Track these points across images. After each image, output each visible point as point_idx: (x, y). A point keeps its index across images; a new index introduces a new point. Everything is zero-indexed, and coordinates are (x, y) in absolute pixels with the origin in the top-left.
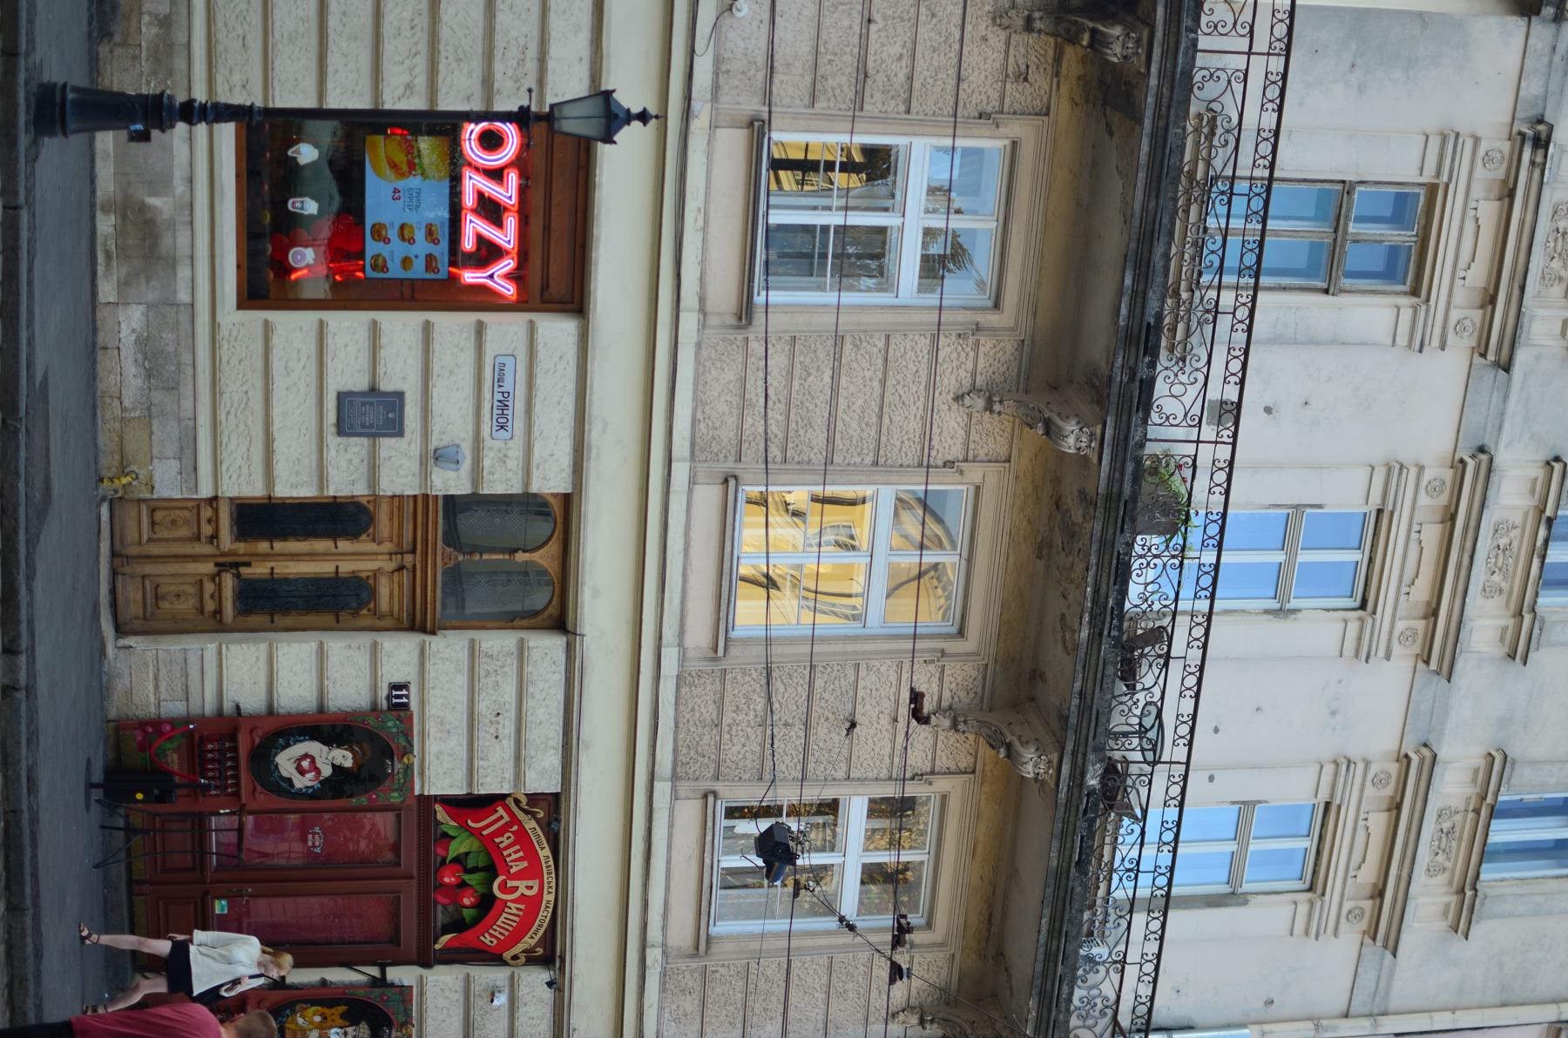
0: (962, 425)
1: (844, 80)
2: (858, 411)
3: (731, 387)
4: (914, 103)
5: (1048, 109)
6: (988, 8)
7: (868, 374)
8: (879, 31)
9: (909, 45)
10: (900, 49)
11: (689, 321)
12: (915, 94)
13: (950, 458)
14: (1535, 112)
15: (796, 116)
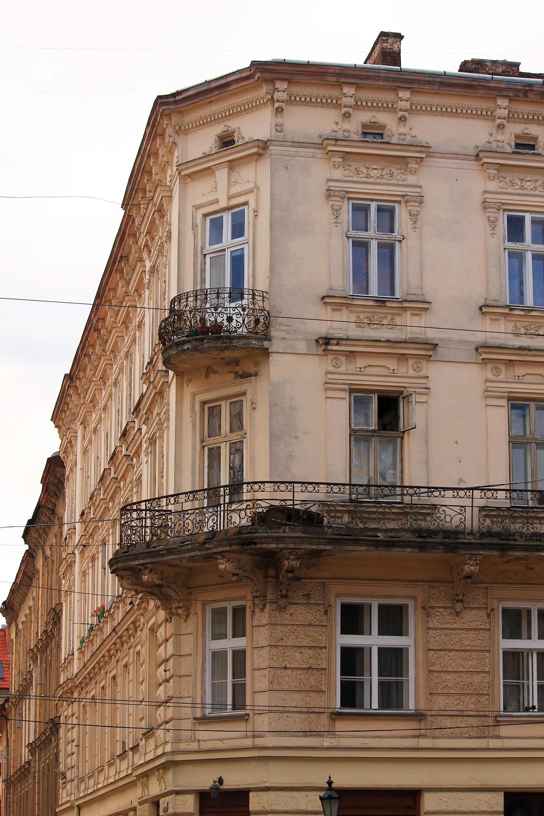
0: (470, 611)
1: (312, 678)
2: (464, 661)
3: (453, 721)
4: (322, 645)
5: (321, 583)
6: (277, 614)
7: (446, 658)
8: (289, 663)
9: (295, 649)
10: (298, 653)
11: (424, 743)
12: (317, 645)
13: (486, 616)
14: (314, 344)
15: (330, 699)
